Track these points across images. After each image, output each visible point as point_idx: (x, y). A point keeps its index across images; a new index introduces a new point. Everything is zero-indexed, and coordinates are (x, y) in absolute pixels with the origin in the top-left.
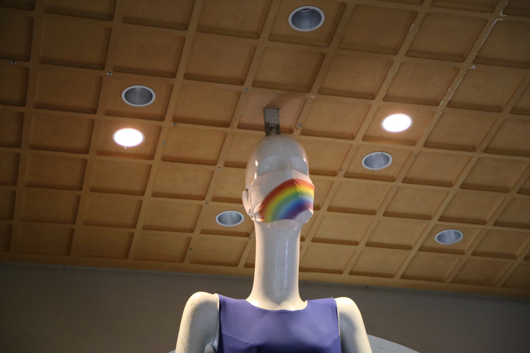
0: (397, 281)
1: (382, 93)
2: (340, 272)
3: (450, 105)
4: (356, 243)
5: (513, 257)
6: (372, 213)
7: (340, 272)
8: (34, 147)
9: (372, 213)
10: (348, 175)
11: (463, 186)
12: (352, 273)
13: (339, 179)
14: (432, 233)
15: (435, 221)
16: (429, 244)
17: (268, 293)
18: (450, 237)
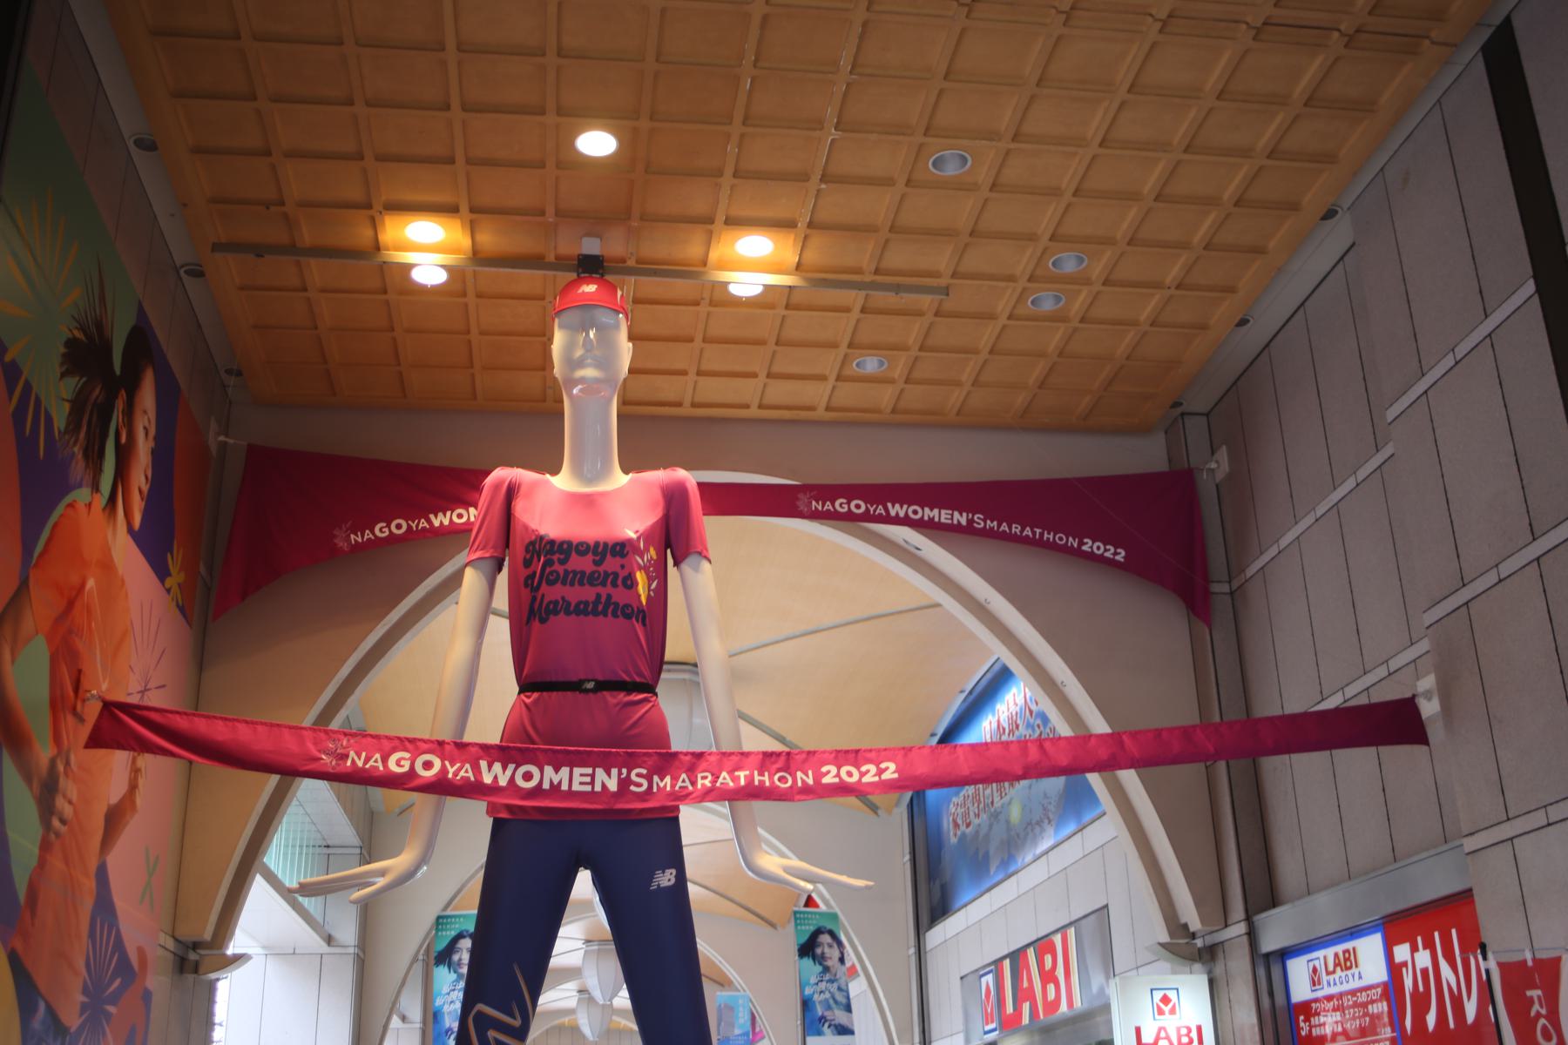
0: (820, 413)
1: (720, 217)
2: (747, 406)
3: (811, 225)
4: (755, 375)
5: (958, 384)
6: (760, 342)
7: (747, 406)
8: (324, 291)
9: (760, 342)
10: (712, 303)
11: (863, 310)
12: (760, 407)
13: (703, 309)
14: (845, 360)
15: (843, 349)
16: (847, 372)
17: (579, 473)
18: (871, 365)
